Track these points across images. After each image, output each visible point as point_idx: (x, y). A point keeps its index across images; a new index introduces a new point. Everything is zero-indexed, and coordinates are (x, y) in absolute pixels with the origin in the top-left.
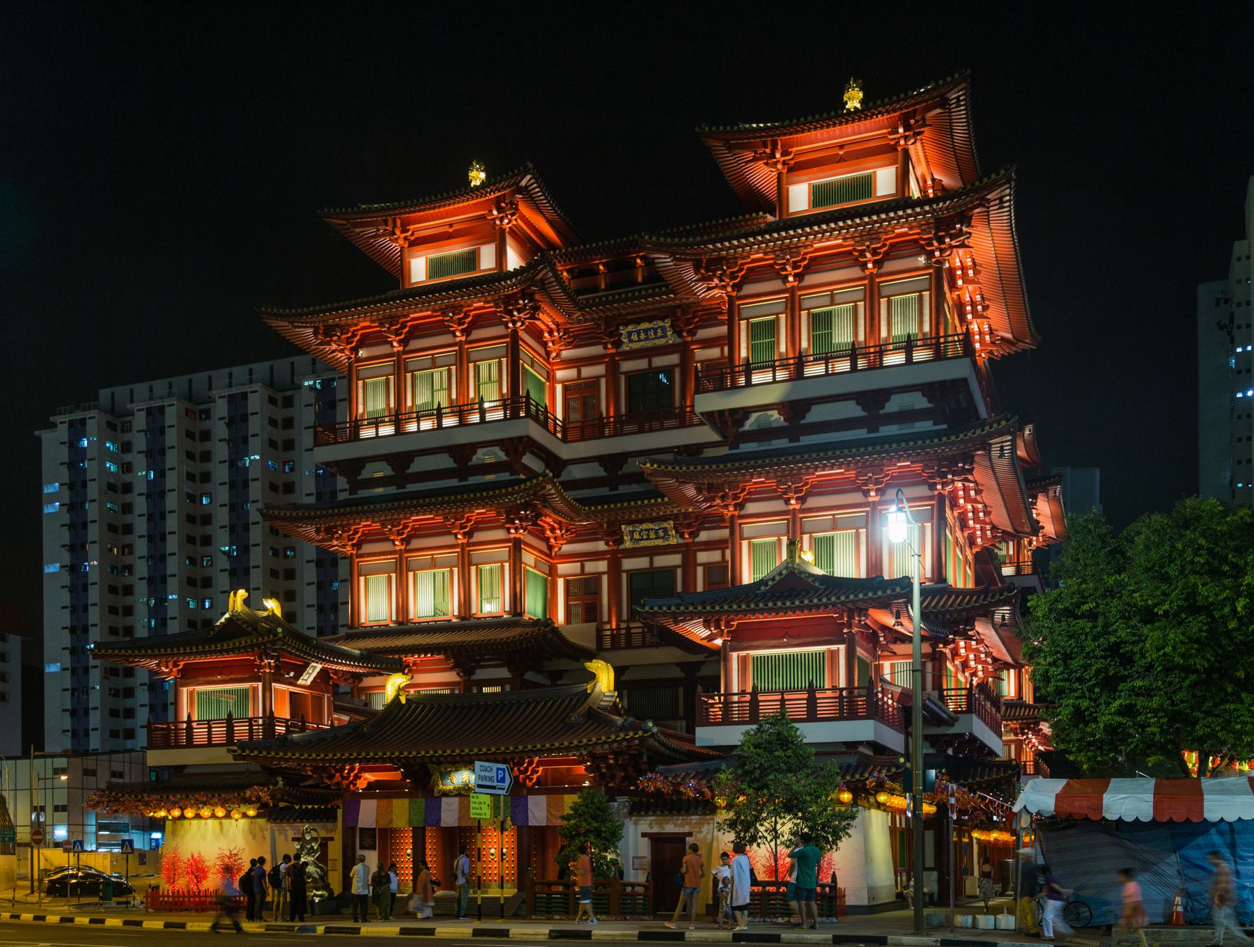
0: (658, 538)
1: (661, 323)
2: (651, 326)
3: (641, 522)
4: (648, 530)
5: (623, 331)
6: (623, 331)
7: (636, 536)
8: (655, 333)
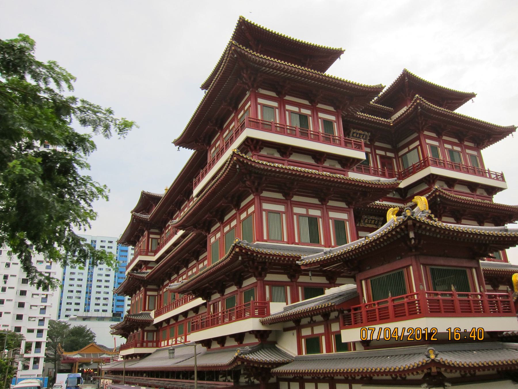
0: (374, 224)
1: (366, 133)
2: (363, 133)
3: (371, 215)
4: (372, 220)
5: (353, 131)
6: (353, 131)
7: (366, 221)
8: (363, 137)
